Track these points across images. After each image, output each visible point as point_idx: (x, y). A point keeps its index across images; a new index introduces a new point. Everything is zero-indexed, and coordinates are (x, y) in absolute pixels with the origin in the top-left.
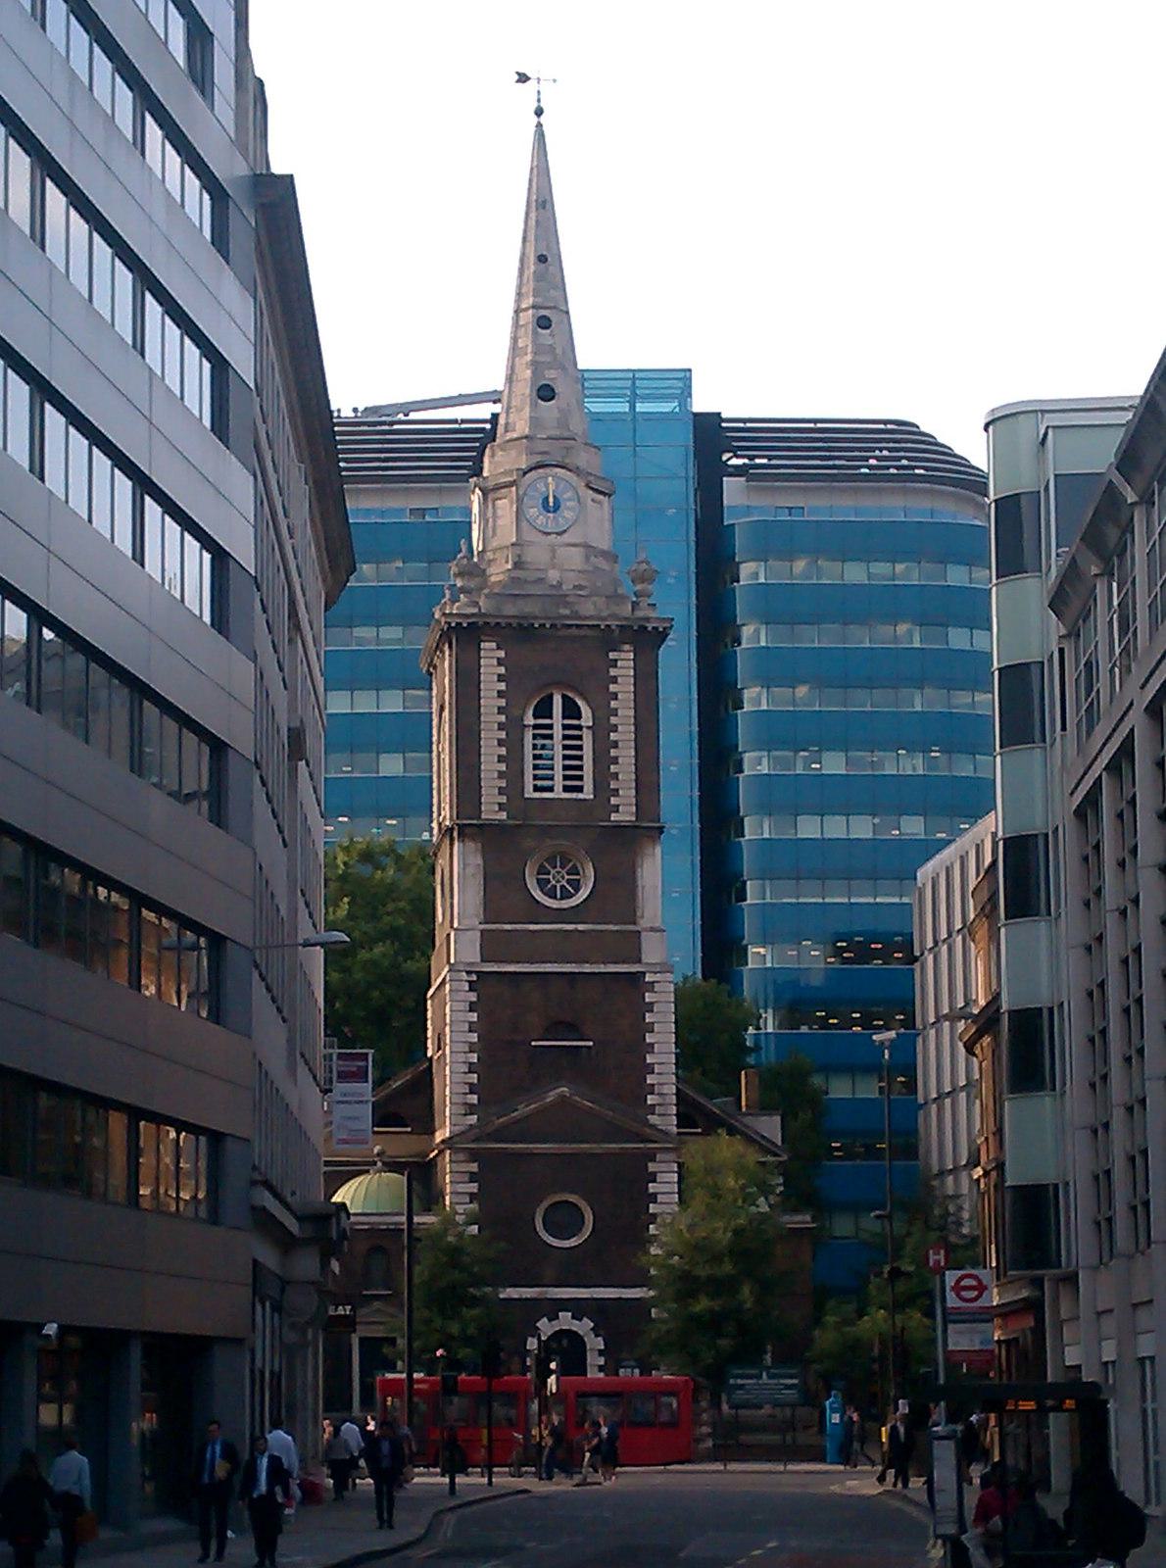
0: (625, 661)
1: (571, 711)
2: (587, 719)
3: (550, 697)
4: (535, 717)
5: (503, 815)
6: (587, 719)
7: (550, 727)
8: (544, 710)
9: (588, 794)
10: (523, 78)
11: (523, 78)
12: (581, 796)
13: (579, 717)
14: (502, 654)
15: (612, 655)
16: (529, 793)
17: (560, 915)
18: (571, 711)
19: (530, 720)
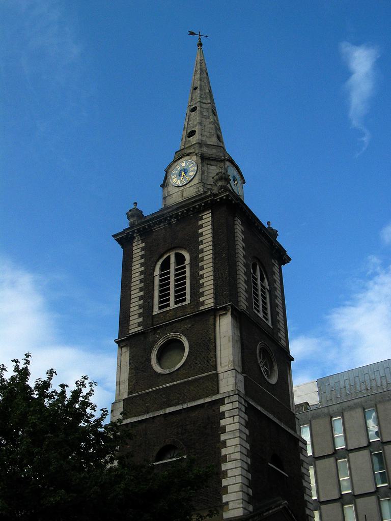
0: (206, 223)
1: (180, 259)
2: (187, 261)
3: (169, 258)
4: (162, 269)
5: (141, 328)
6: (187, 261)
7: (169, 273)
8: (166, 266)
9: (188, 302)
10: (192, 33)
11: (192, 33)
12: (185, 303)
13: (183, 259)
14: (143, 245)
15: (200, 223)
16: (156, 311)
17: (171, 376)
18: (180, 259)
19: (157, 272)
